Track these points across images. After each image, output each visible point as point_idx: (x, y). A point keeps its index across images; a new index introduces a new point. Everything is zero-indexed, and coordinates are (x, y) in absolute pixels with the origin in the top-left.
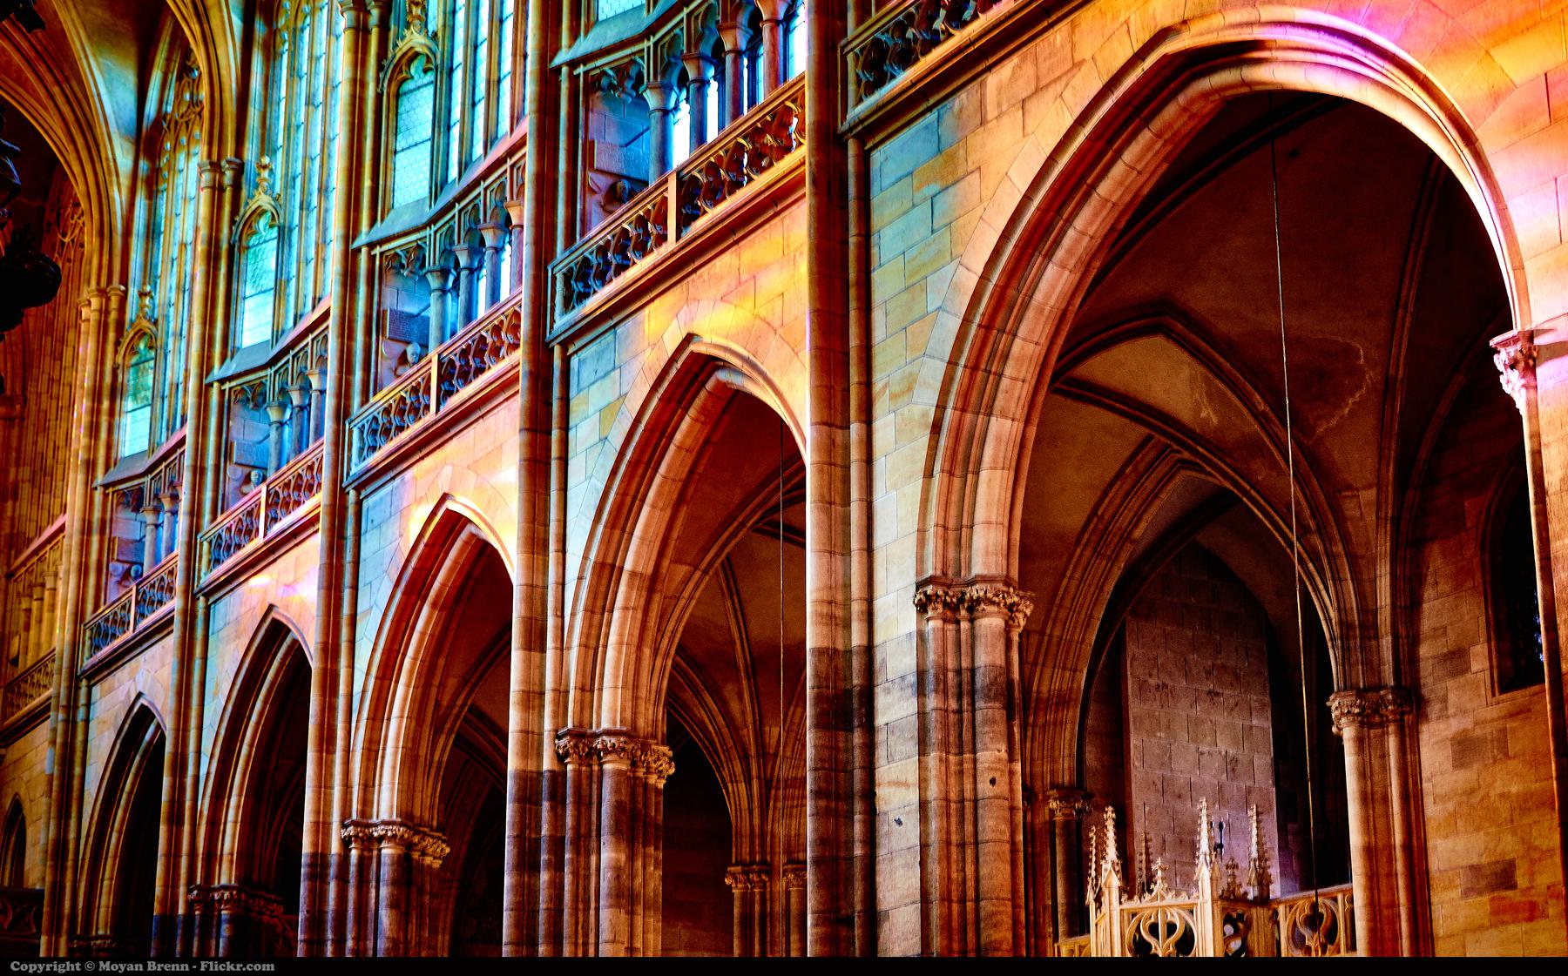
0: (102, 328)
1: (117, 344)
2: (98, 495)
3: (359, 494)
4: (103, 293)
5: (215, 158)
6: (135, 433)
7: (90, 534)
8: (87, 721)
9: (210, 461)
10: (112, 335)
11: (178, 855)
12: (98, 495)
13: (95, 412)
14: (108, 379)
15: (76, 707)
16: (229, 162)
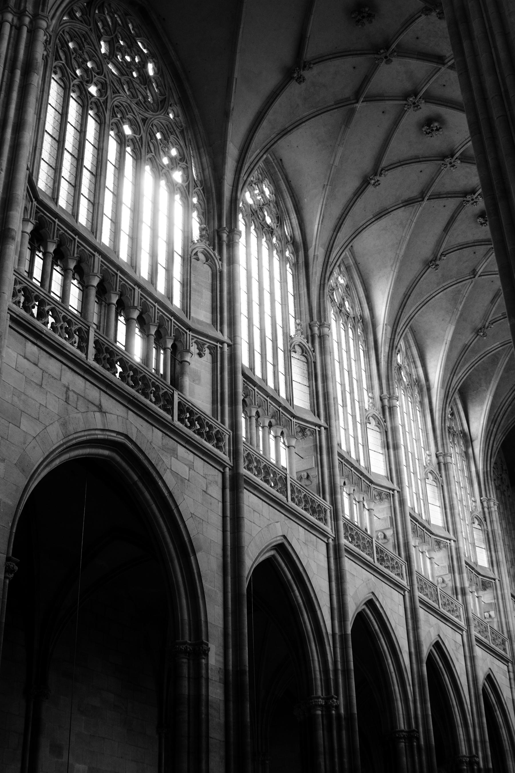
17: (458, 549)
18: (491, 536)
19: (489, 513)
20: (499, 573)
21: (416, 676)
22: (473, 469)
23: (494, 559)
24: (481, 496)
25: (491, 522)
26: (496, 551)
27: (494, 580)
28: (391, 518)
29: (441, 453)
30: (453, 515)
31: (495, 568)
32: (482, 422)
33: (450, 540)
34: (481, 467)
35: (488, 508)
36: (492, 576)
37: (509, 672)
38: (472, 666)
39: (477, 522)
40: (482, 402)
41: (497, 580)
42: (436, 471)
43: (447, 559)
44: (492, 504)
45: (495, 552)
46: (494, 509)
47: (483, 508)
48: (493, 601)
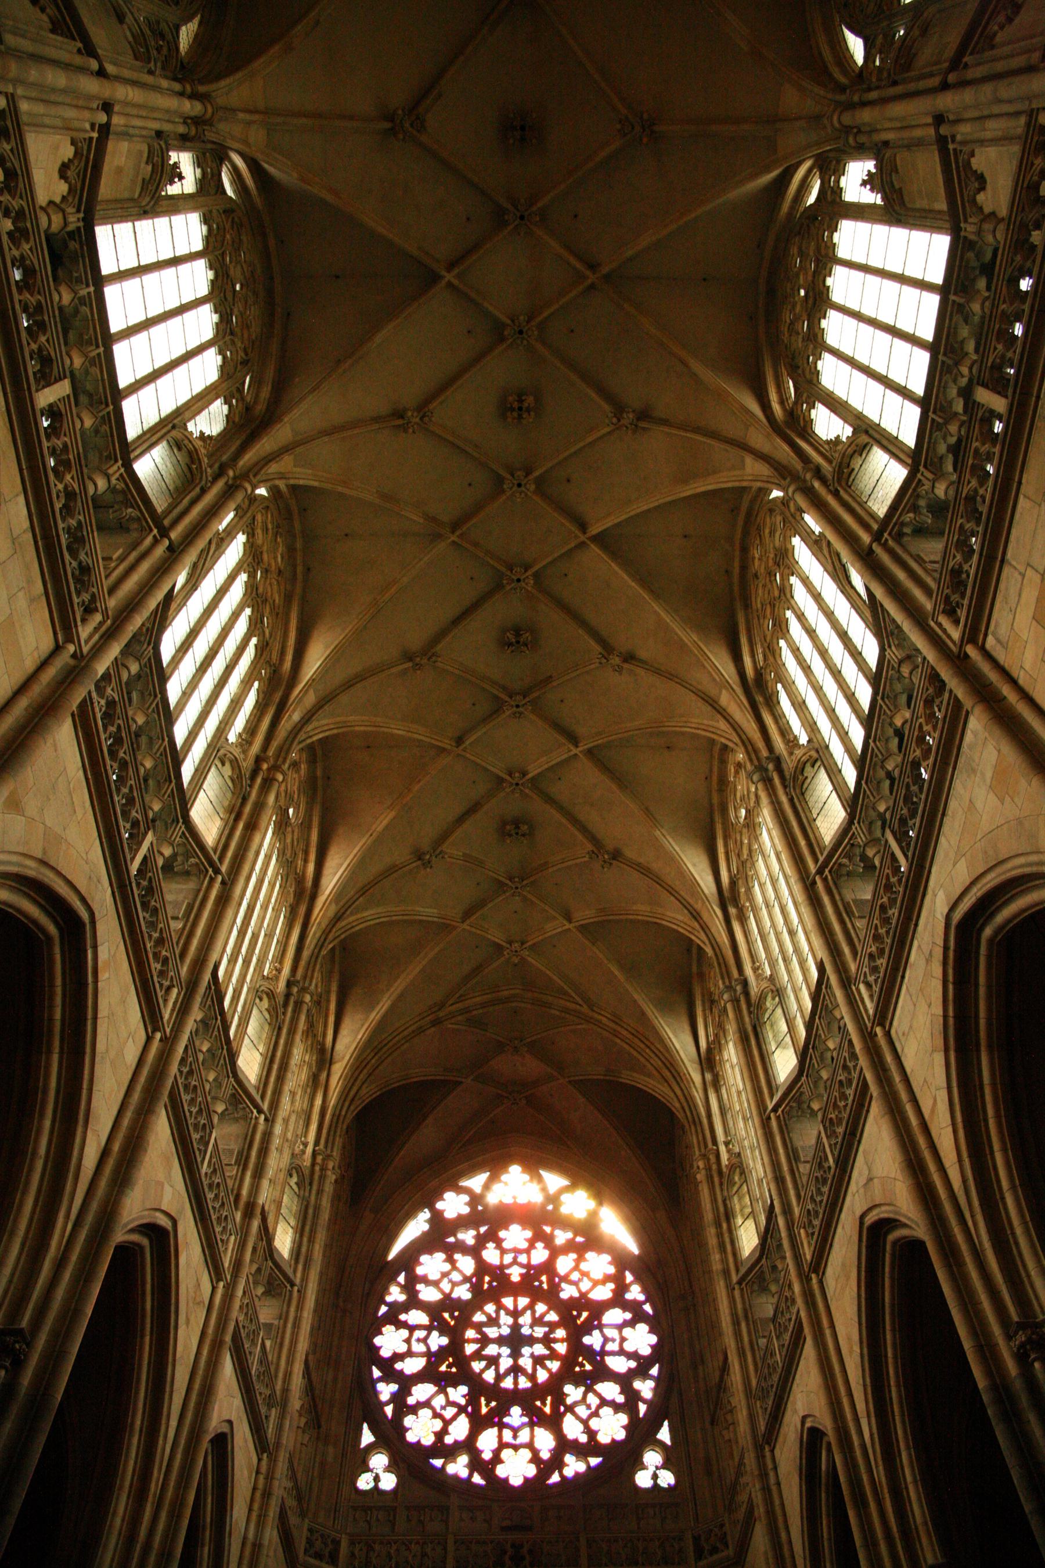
0: (710, 1178)
1: (721, 1184)
2: (737, 1293)
3: (884, 1027)
4: (704, 1156)
5: (727, 983)
6: (748, 1239)
7: (739, 1324)
8: (778, 1484)
9: (785, 1168)
10: (716, 1180)
11: (876, 1545)
12: (737, 1293)
13: (720, 1235)
14: (722, 1209)
15: (767, 1475)
16: (736, 980)
17: (267, 1135)
18: (311, 1211)
19: (320, 1177)
20: (305, 1279)
21: (94, 1206)
22: (318, 1102)
23: (304, 1249)
24: (317, 1142)
25: (320, 1192)
26: (311, 1240)
27: (293, 1285)
28: (190, 907)
29: (298, 982)
30: (281, 1079)
31: (300, 1267)
32: (359, 1037)
33: (260, 1111)
34: (332, 1102)
35: (323, 1169)
36: (291, 1275)
37: (258, 1472)
38: (209, 1363)
39: (295, 1179)
40: (371, 1007)
41: (296, 1288)
42: (280, 999)
43: (240, 1141)
44: (331, 1165)
45: (309, 1241)
46: (331, 1177)
47: (313, 1164)
48: (276, 1322)
